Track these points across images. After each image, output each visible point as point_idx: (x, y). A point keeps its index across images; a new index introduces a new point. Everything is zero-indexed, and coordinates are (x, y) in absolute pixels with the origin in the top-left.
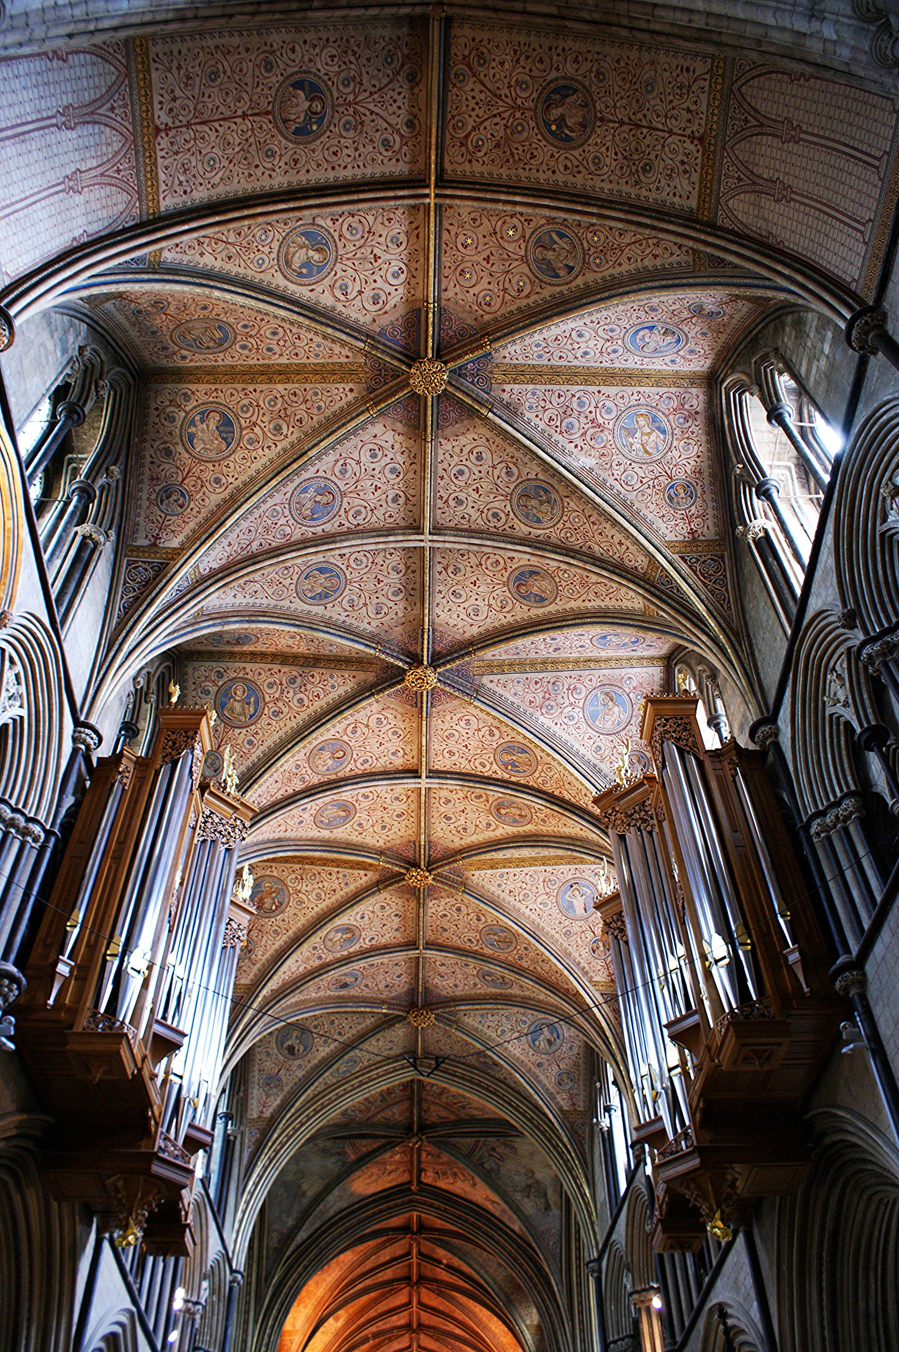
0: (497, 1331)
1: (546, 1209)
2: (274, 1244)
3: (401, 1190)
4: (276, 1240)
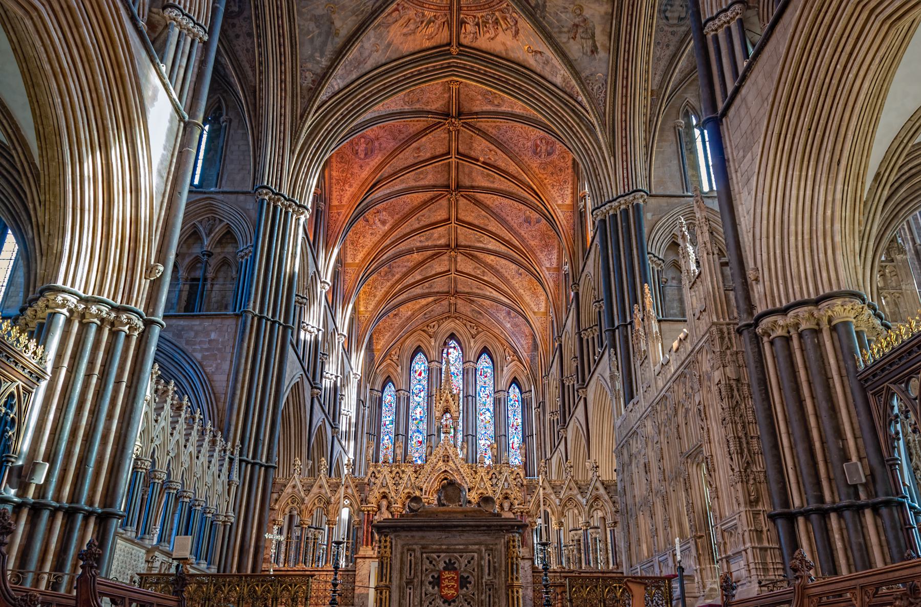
0: (526, 236)
2: (308, 83)
3: (440, 51)
4: (309, 80)
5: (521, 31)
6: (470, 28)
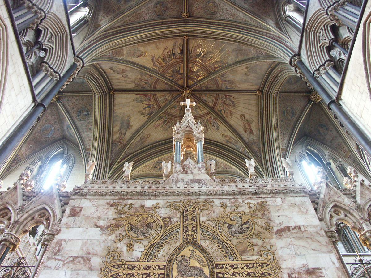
5: (151, 61)
6: (178, 51)
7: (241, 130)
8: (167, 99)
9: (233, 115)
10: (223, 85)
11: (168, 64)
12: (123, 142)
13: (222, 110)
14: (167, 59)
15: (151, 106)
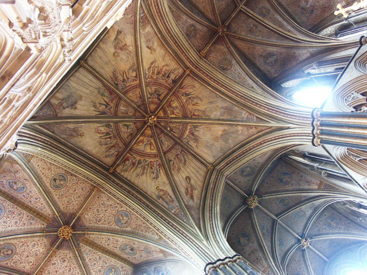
1: (121, 32)
5: (150, 63)
6: (173, 77)
7: (183, 190)
8: (129, 113)
9: (180, 172)
10: (188, 138)
11: (158, 81)
12: (58, 113)
13: (171, 160)
14: (161, 75)
15: (109, 107)
